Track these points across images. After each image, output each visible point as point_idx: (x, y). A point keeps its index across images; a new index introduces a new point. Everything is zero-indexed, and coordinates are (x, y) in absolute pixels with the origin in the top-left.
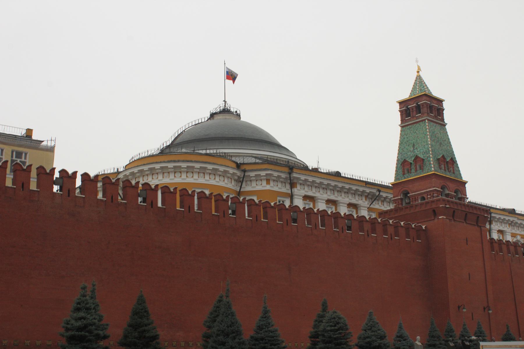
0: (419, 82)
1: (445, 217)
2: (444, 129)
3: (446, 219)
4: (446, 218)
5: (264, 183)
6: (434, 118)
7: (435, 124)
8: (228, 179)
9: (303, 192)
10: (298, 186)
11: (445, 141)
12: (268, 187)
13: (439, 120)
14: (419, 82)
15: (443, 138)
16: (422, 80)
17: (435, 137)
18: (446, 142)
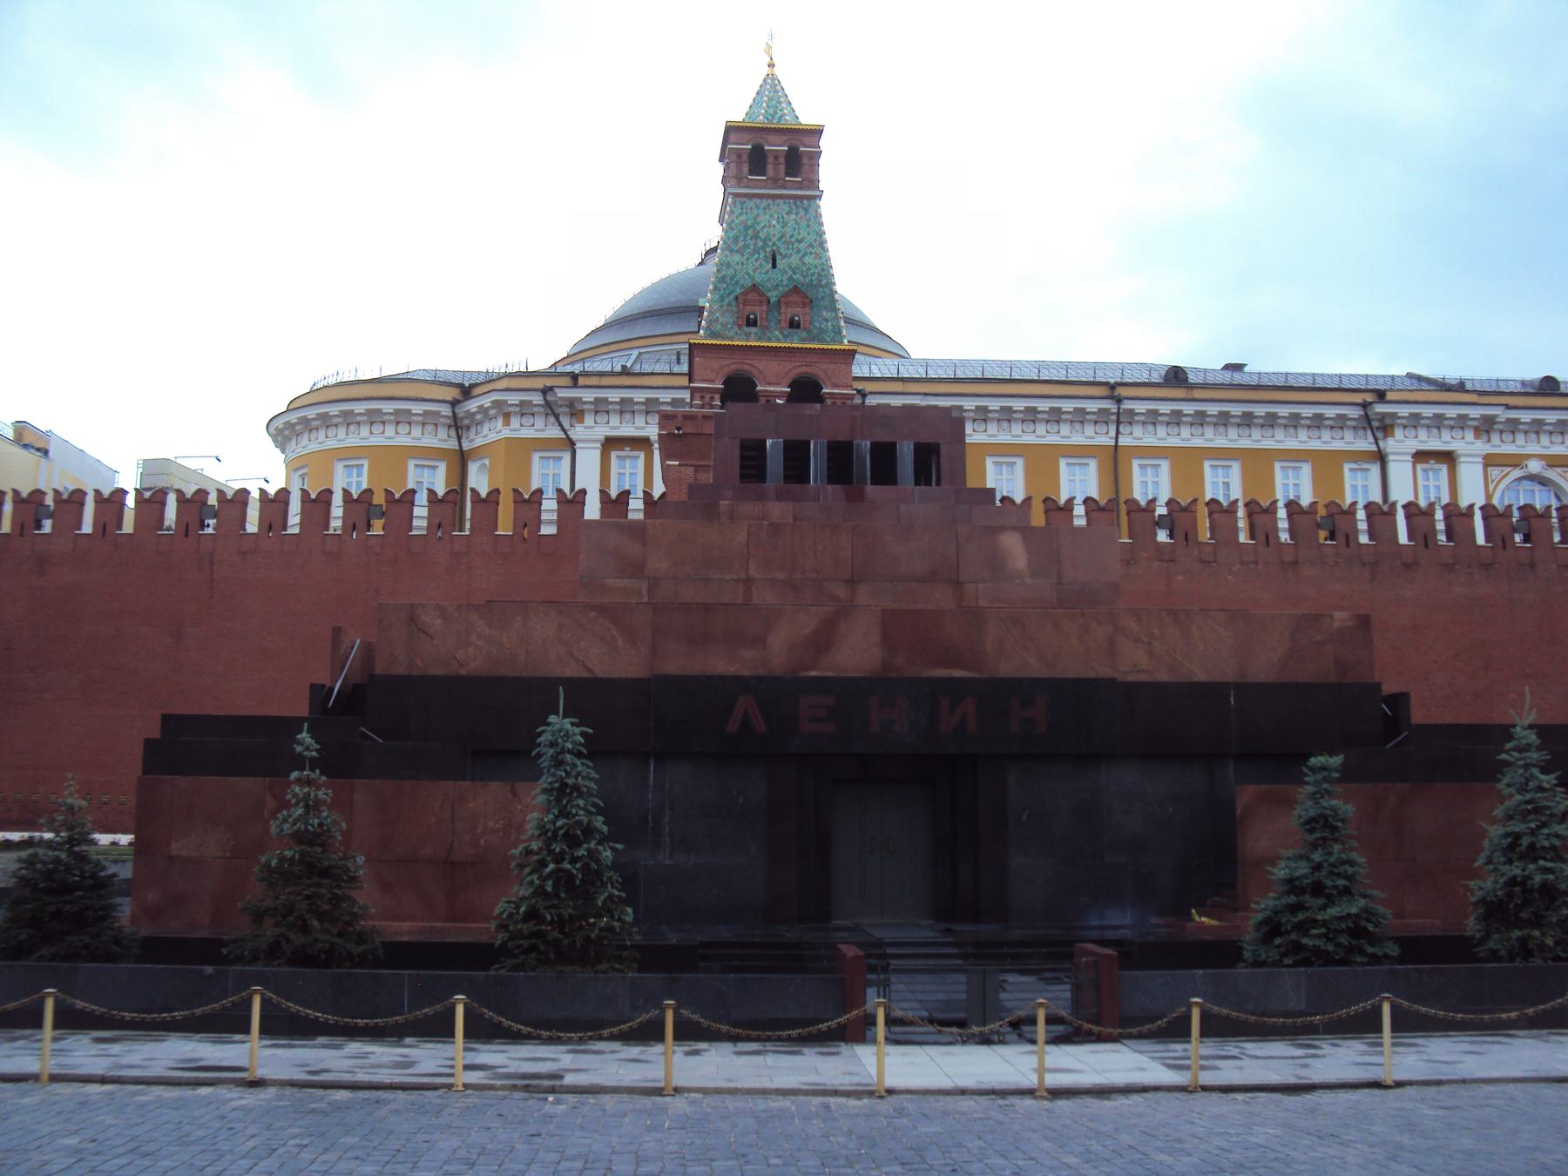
0: (771, 89)
1: (677, 463)
2: (806, 210)
3: (683, 469)
4: (679, 465)
5: (500, 422)
6: (765, 188)
7: (765, 202)
8: (546, 418)
9: (602, 431)
10: (589, 420)
11: (800, 241)
12: (506, 433)
13: (791, 188)
14: (771, 89)
15: (792, 236)
16: (779, 88)
17: (756, 237)
18: (802, 246)
